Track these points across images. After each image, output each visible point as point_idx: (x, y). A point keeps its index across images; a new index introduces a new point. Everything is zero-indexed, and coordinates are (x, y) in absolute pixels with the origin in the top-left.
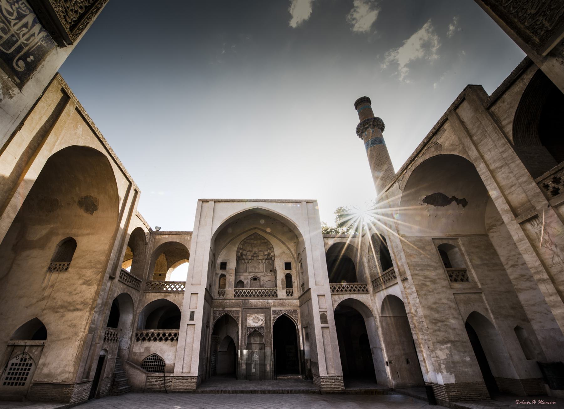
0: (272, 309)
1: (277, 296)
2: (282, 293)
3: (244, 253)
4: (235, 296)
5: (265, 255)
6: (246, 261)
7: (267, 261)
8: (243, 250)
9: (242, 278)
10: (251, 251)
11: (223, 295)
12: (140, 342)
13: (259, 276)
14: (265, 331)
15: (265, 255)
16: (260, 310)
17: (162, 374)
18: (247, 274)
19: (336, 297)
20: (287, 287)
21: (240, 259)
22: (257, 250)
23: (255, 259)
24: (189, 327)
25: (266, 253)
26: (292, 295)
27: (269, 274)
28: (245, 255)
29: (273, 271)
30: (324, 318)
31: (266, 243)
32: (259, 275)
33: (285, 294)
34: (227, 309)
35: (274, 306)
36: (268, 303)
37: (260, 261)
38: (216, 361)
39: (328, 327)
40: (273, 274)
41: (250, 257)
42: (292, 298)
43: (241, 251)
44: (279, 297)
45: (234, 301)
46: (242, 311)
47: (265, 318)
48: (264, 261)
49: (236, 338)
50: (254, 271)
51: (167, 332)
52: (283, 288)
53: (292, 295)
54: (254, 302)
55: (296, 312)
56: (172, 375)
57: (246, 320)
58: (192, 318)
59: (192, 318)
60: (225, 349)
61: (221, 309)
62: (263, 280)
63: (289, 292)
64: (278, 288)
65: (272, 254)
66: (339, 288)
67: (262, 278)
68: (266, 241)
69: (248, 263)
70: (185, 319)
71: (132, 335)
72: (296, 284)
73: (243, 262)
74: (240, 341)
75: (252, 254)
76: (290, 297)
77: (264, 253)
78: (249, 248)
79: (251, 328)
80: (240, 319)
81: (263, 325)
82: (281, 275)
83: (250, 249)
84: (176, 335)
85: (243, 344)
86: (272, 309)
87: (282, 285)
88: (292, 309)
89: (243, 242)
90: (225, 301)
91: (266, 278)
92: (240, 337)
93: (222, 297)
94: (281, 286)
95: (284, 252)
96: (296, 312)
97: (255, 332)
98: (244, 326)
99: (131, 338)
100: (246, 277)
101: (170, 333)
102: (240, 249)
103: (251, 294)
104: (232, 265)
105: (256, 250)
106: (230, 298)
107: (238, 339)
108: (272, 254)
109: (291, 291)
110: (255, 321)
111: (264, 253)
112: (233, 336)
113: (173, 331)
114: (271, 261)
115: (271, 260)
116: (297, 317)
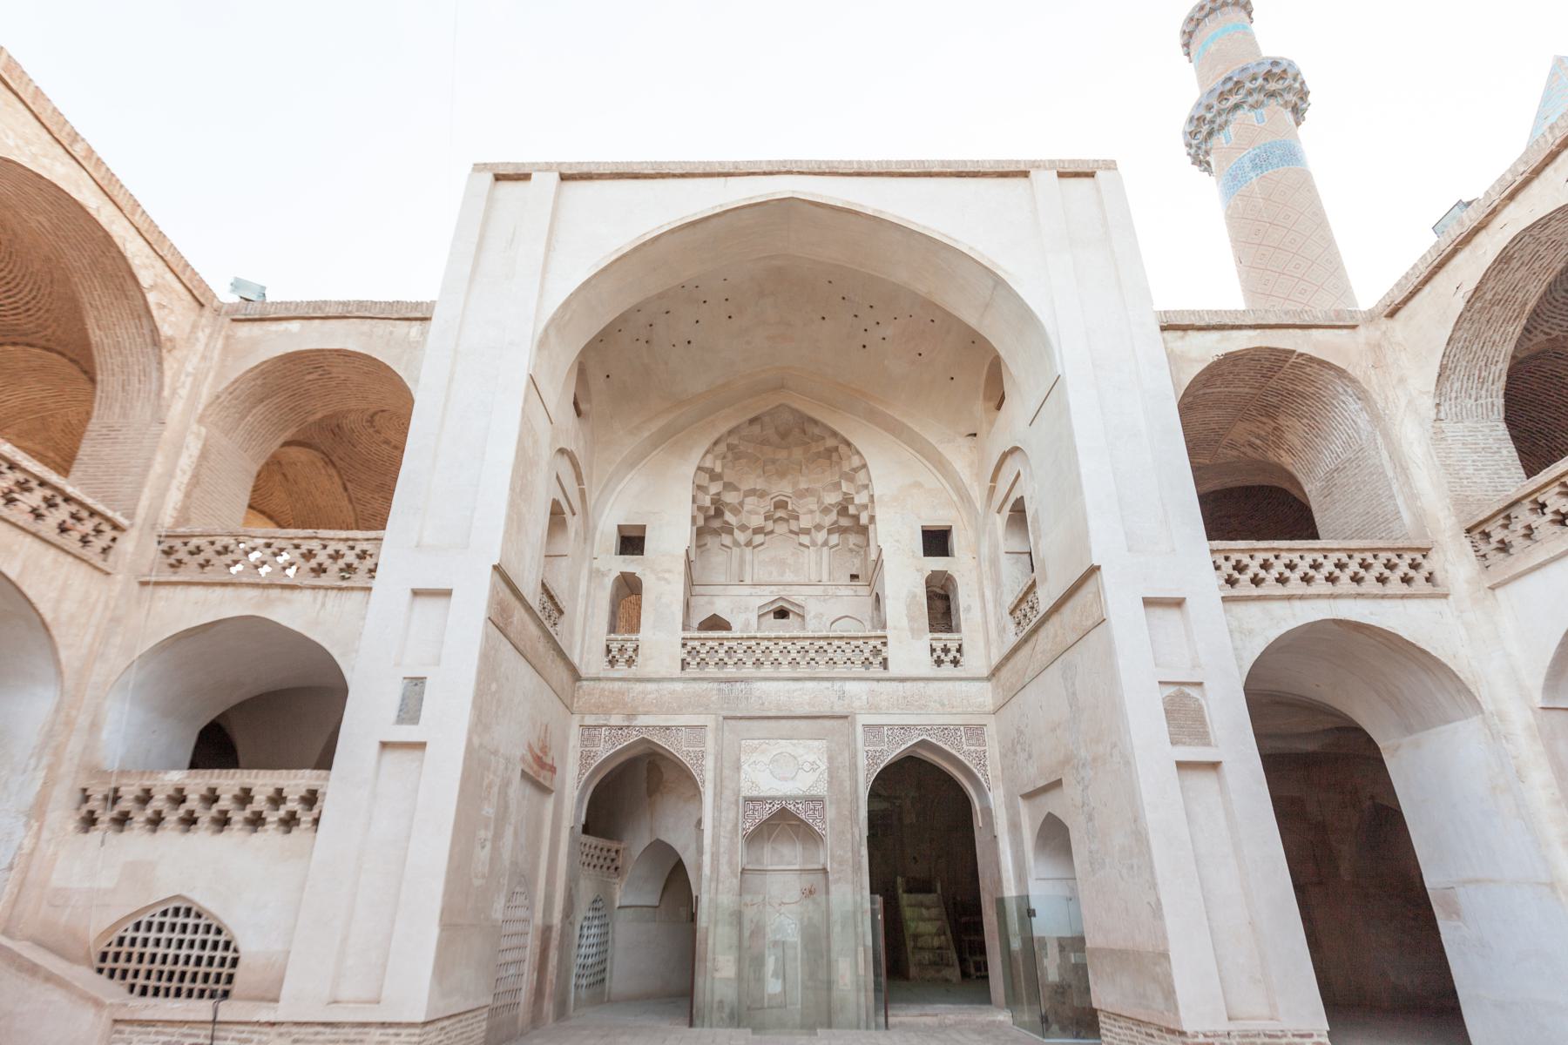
0: (862, 720)
1: (884, 664)
2: (910, 646)
3: (730, 498)
4: (684, 664)
5: (826, 510)
6: (741, 537)
7: (834, 539)
8: (729, 486)
9: (721, 607)
10: (762, 494)
11: (630, 662)
12: (95, 835)
13: (798, 600)
14: (831, 813)
15: (826, 510)
16: (803, 724)
17: (201, 1009)
18: (746, 590)
19: (1251, 614)
20: (933, 629)
21: (711, 523)
22: (789, 490)
23: (781, 528)
24: (391, 757)
25: (832, 498)
26: (955, 662)
27: (844, 591)
28: (736, 511)
29: (866, 577)
30: (1184, 714)
31: (830, 452)
32: (797, 595)
33: (928, 659)
34: (642, 720)
35: (873, 708)
36: (842, 695)
37: (805, 539)
38: (604, 943)
39: (1215, 766)
40: (865, 591)
41: (757, 521)
42: (957, 672)
43: (715, 488)
44: (894, 670)
45: (679, 686)
46: (719, 729)
47: (831, 759)
48: (821, 536)
49: (693, 847)
50: (775, 578)
51: (263, 782)
52: (915, 633)
53: (955, 662)
54: (774, 692)
55: (975, 731)
56: (265, 1015)
57: (738, 768)
58: (410, 710)
59: (410, 710)
60: (653, 900)
61: (616, 720)
62: (819, 616)
63: (946, 650)
64: (889, 633)
65: (861, 499)
66: (1265, 566)
67: (812, 608)
68: (830, 442)
69: (748, 544)
70: (364, 721)
71: (48, 784)
72: (976, 614)
73: (726, 539)
74: (707, 859)
75: (767, 505)
76: (947, 670)
77: (819, 501)
78: (753, 481)
79: (762, 800)
80: (709, 763)
81: (821, 790)
82: (905, 574)
83: (760, 484)
84: (311, 799)
85: (724, 869)
86: (862, 720)
87: (911, 619)
88: (958, 720)
89: (722, 448)
90: (639, 687)
91: (829, 608)
92: (707, 840)
93: (621, 670)
94: (905, 622)
95: (918, 485)
96: (975, 731)
97: (782, 823)
98: (728, 793)
99: (37, 811)
100: (742, 607)
101: (279, 791)
102: (715, 477)
103: (758, 653)
104: (671, 535)
105: (783, 488)
106: (663, 673)
107: (700, 851)
108: (861, 499)
109: (953, 646)
110: (786, 769)
111: (819, 501)
112: (679, 840)
113: (296, 782)
114: (853, 539)
115: (853, 525)
116: (981, 758)
